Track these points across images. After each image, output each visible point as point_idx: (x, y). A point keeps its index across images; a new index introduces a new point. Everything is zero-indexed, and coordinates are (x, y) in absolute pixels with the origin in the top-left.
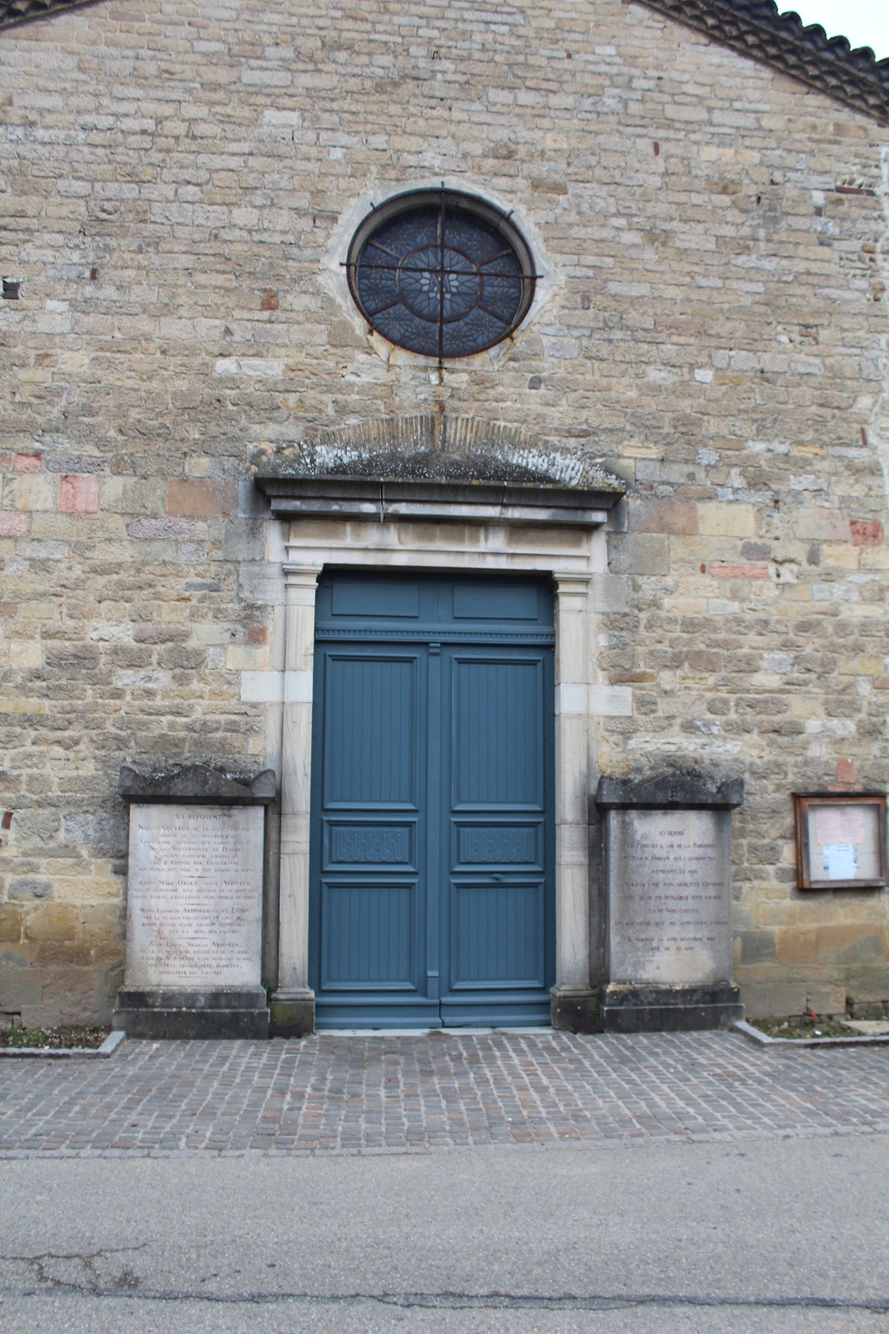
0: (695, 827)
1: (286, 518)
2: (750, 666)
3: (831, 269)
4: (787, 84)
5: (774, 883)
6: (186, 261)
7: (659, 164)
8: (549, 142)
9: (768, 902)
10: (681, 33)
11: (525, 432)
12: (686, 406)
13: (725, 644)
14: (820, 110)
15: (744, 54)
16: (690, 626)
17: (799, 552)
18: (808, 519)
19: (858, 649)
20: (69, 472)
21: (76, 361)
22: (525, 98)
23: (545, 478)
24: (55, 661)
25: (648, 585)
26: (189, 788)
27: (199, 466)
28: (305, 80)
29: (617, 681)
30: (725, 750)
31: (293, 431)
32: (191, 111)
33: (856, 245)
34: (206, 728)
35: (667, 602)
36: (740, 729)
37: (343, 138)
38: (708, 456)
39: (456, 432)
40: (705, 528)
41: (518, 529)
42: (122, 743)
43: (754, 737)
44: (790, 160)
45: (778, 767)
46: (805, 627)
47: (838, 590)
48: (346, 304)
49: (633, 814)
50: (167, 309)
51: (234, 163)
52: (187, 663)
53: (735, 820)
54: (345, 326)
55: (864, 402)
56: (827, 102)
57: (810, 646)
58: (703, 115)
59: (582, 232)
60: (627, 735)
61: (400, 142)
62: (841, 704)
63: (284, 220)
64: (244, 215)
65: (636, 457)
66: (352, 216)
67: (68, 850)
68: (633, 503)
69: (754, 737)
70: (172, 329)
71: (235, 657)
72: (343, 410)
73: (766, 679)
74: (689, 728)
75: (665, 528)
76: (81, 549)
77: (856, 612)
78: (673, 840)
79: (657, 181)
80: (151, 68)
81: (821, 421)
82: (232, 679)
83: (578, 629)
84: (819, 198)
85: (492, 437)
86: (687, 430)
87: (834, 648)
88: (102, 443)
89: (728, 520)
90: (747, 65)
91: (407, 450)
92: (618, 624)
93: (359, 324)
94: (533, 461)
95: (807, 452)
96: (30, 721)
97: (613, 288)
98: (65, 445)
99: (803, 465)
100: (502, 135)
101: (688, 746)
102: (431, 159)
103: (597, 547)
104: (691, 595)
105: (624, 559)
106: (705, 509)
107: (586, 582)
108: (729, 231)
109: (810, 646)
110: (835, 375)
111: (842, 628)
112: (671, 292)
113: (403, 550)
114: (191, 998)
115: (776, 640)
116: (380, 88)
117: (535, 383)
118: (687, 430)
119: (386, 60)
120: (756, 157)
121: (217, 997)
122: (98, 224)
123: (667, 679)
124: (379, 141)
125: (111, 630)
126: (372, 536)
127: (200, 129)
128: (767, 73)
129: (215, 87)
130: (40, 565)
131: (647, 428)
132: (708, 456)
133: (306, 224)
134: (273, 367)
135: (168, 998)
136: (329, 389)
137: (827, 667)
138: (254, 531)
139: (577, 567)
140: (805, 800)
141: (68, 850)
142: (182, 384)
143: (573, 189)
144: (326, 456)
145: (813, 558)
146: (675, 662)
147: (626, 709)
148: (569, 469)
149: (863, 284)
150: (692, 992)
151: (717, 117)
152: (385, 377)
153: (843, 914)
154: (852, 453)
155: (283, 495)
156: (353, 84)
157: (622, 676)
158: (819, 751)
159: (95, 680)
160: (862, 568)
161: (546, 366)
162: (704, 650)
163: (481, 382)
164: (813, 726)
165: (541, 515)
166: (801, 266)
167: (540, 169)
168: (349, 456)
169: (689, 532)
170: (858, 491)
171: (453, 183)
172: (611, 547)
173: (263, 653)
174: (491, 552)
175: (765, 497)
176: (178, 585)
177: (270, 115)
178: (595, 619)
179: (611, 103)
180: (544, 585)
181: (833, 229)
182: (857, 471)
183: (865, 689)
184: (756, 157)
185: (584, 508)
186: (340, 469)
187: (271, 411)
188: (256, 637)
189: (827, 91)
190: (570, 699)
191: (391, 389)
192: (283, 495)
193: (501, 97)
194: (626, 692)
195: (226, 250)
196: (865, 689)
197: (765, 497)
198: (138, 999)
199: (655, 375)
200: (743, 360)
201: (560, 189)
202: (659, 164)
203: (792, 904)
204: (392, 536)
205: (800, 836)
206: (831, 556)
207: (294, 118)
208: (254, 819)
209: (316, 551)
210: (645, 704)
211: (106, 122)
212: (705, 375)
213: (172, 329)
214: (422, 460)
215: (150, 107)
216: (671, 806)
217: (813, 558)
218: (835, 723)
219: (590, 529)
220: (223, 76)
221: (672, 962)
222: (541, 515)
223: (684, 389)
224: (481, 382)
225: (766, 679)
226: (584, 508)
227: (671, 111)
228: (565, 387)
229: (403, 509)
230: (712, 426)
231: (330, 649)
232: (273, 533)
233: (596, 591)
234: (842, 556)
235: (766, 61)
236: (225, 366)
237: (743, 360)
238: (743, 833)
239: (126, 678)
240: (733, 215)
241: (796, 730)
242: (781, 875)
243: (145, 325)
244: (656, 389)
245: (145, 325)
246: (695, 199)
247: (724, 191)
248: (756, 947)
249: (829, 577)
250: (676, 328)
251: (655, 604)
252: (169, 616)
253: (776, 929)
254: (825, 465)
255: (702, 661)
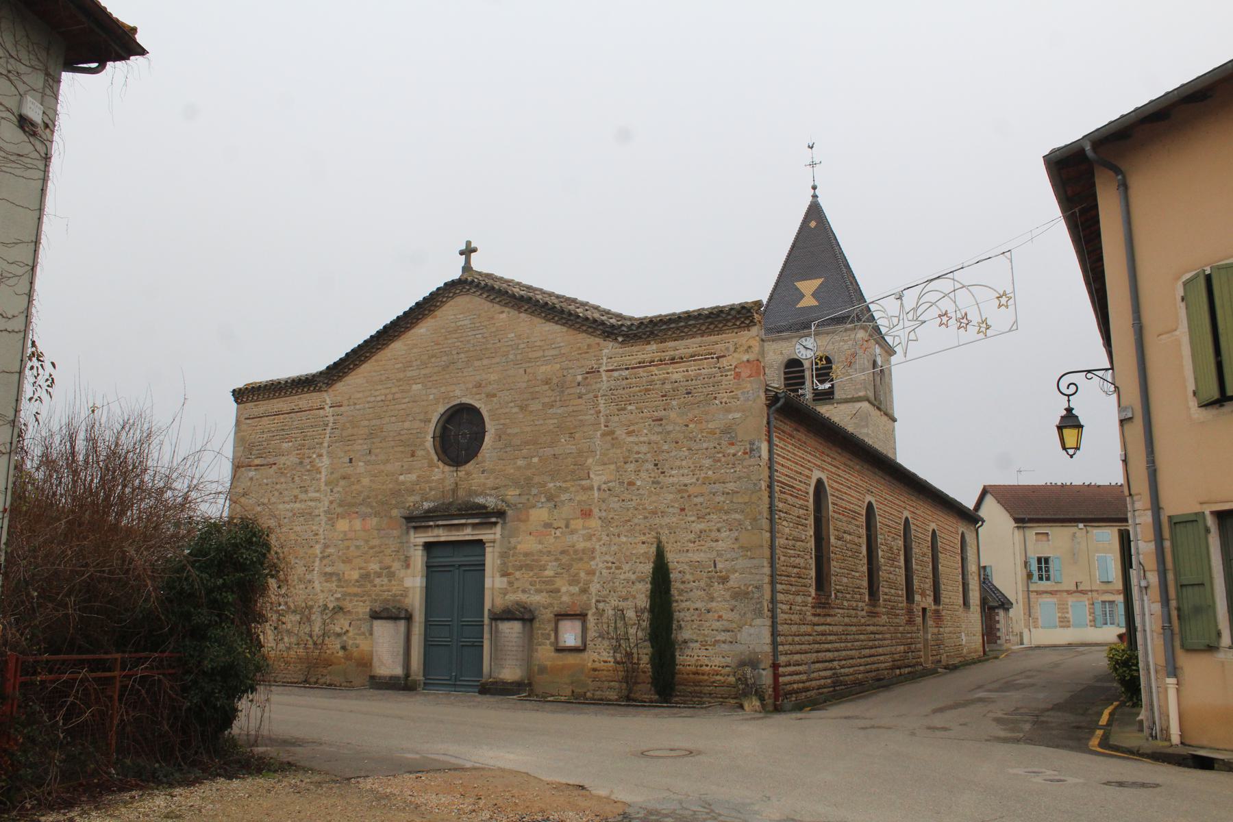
0: (516, 626)
1: (415, 528)
2: (543, 568)
3: (580, 408)
4: (571, 332)
5: (549, 647)
6: (392, 443)
7: (526, 378)
8: (493, 377)
9: (545, 654)
10: (536, 320)
11: (480, 490)
12: (529, 473)
13: (536, 561)
14: (584, 340)
15: (557, 323)
16: (526, 555)
17: (562, 524)
18: (566, 511)
19: (581, 559)
20: (364, 517)
21: (366, 481)
22: (485, 362)
23: (485, 507)
24: (362, 576)
25: (513, 540)
26: (384, 614)
27: (395, 512)
28: (423, 372)
29: (502, 576)
30: (536, 599)
31: (418, 498)
32: (394, 390)
33: (591, 395)
34: (395, 595)
35: (519, 547)
36: (539, 591)
37: (434, 391)
38: (534, 491)
39: (461, 493)
40: (531, 518)
41: (474, 526)
42: (376, 601)
43: (544, 594)
44: (570, 365)
45: (551, 605)
46: (563, 552)
47: (575, 537)
48: (432, 452)
49: (499, 623)
50: (388, 461)
51: (404, 406)
52: (391, 575)
53: (536, 624)
54: (432, 460)
55: (590, 461)
56: (584, 335)
57: (565, 559)
58: (540, 353)
59: (500, 411)
60: (505, 594)
61: (449, 388)
62: (574, 581)
63: (417, 424)
64: (407, 425)
65: (512, 494)
66: (435, 420)
67: (364, 634)
68: (510, 512)
69: (544, 594)
70: (389, 468)
71: (402, 573)
72: (431, 489)
73: (549, 573)
74: (524, 591)
75: (520, 520)
76: (367, 541)
77: (581, 545)
78: (511, 630)
79: (524, 385)
80: (383, 378)
81: (573, 472)
82: (402, 580)
83: (491, 559)
84: (579, 378)
85: (471, 493)
86: (529, 482)
87: (573, 560)
88: (372, 507)
89: (539, 514)
90: (558, 328)
91: (446, 501)
92: (504, 555)
93: (435, 458)
94: (480, 500)
95: (568, 484)
96: (356, 595)
97: (509, 431)
98: (363, 509)
99: (566, 490)
100: (478, 378)
101: (523, 597)
102: (458, 393)
103: (498, 529)
104: (527, 544)
105: (506, 532)
106: (533, 512)
107: (494, 542)
108: (547, 400)
109: (565, 559)
110: (580, 452)
111: (576, 552)
112: (528, 429)
113: (443, 536)
114: (385, 677)
115: (553, 558)
116: (444, 369)
117: (483, 472)
118: (529, 482)
119: (444, 358)
120: (558, 366)
121: (391, 677)
122: (371, 435)
123: (518, 574)
124: (443, 389)
125: (374, 567)
126: (436, 532)
127: (397, 396)
128: (565, 329)
129: (399, 380)
130: (357, 547)
131: (516, 484)
132: (534, 491)
133: (422, 425)
134: (413, 477)
135: (380, 678)
136: (427, 482)
137: (570, 566)
138: (408, 533)
139: (492, 537)
140: (561, 616)
141: (364, 634)
142: (391, 486)
143: (499, 394)
144: (426, 505)
145: (567, 526)
146: (520, 568)
147: (505, 586)
148: (491, 502)
149: (592, 412)
150: (512, 683)
151: (547, 353)
152: (442, 476)
153: (571, 659)
154: (583, 482)
155: (416, 521)
156: (436, 369)
157: (504, 574)
158: (565, 599)
159: (371, 582)
160: (584, 528)
161: (487, 465)
162: (531, 564)
163: (468, 474)
164: (564, 589)
165: (477, 521)
166: (571, 409)
167: (490, 389)
168: (431, 505)
169: (526, 520)
170: (585, 498)
171: (464, 400)
172: (502, 528)
173: (409, 571)
174: (467, 534)
175: (551, 505)
176: (388, 551)
177: (414, 387)
178: (496, 554)
179: (511, 357)
180: (480, 543)
181: (584, 391)
182: (585, 489)
183: (582, 574)
184: (558, 366)
185: (489, 516)
186: (429, 511)
187: (411, 492)
188: (408, 566)
189: (585, 331)
190: (488, 583)
191: (443, 480)
192: (416, 521)
193: (477, 363)
194: (505, 579)
195: (403, 438)
196: (582, 574)
197: (551, 505)
198: (373, 677)
199: (520, 463)
200: (549, 451)
201: (494, 395)
202: (526, 378)
203: (553, 654)
204: (440, 531)
205: (556, 630)
206: (573, 524)
207: (420, 386)
208: (402, 625)
209: (420, 538)
210: (510, 583)
211: (373, 399)
212: (535, 460)
213: (389, 468)
214: (451, 504)
215: (383, 391)
216: (509, 619)
217: (567, 526)
218: (571, 588)
219: (495, 524)
220: (401, 375)
221: (510, 672)
222: (477, 521)
223: (529, 466)
224: (468, 474)
225: (549, 573)
226: (489, 516)
227: (530, 355)
228: (493, 471)
229: (440, 523)
230: (536, 479)
231: (431, 570)
232: (412, 532)
233: (497, 545)
234: (577, 524)
235: (563, 325)
236: (402, 478)
237: (549, 451)
238: (539, 628)
239: (377, 581)
240: (549, 393)
241: (558, 591)
242: (551, 644)
243: (382, 467)
244: (519, 468)
245: (382, 467)
246: (537, 389)
247: (547, 383)
248: (543, 670)
249: (572, 533)
250: (527, 443)
251: (515, 548)
252: (388, 561)
253: (548, 663)
254: (572, 489)
255: (529, 567)
